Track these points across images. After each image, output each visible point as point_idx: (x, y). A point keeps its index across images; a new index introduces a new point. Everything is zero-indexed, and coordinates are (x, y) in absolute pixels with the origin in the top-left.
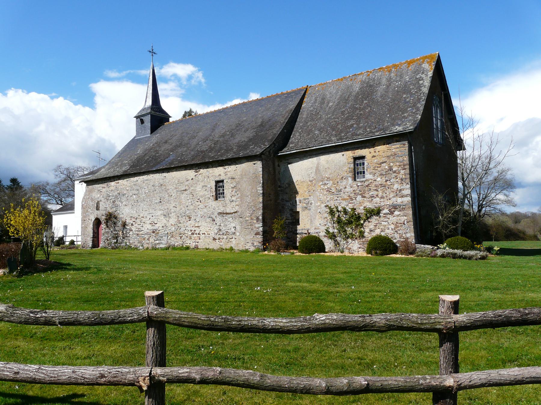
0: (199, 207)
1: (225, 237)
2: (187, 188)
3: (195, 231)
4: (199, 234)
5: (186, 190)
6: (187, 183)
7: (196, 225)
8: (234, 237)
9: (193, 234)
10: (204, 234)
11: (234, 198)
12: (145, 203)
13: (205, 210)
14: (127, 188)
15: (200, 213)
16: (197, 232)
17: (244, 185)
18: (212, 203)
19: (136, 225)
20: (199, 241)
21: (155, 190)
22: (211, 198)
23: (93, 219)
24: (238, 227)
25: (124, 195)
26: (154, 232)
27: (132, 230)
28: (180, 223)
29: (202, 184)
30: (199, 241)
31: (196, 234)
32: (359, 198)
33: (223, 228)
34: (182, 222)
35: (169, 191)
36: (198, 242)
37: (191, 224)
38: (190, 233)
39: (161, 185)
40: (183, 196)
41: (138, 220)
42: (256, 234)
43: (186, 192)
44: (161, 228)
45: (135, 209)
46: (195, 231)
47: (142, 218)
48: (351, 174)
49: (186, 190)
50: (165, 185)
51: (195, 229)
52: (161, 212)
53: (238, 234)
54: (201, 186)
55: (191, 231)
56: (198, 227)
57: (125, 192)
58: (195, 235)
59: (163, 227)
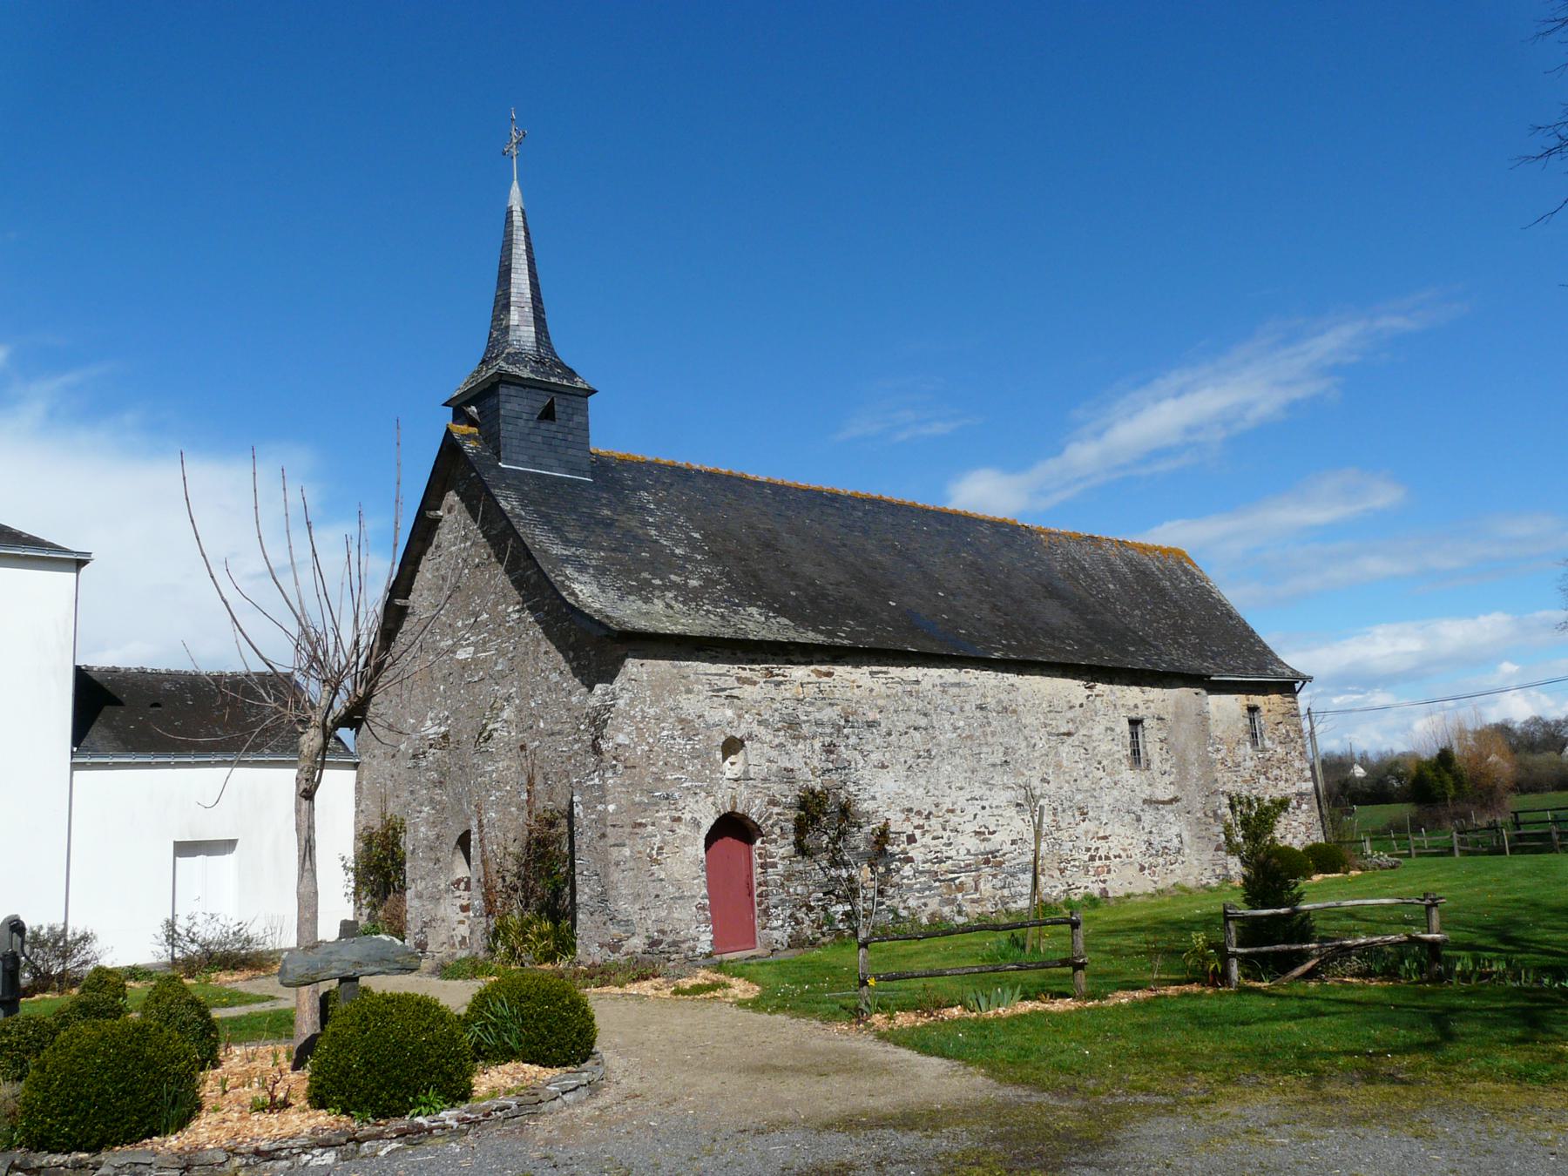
0: (1103, 783)
1: (1161, 860)
2: (1071, 727)
4: (1107, 858)
5: (1069, 734)
6: (1070, 715)
7: (1101, 834)
8: (1181, 858)
9: (1092, 858)
11: (1167, 767)
12: (957, 760)
13: (1116, 793)
14: (881, 702)
15: (1107, 800)
16: (1102, 853)
17: (1182, 739)
18: (1127, 775)
19: (928, 839)
20: (1107, 877)
21: (989, 724)
22: (1125, 761)
23: (708, 823)
24: (1186, 836)
25: (871, 725)
26: (987, 862)
27: (910, 860)
28: (1059, 829)
29: (1104, 723)
30: (1107, 877)
33: (1155, 840)
34: (1063, 825)
35: (1026, 732)
36: (1104, 882)
37: (1087, 832)
38: (1086, 858)
39: (1006, 709)
40: (1064, 750)
41: (933, 820)
43: (1069, 740)
44: (1007, 847)
45: (923, 782)
47: (948, 816)
48: (1248, 737)
49: (1069, 734)
52: (1010, 794)
53: (1187, 851)
54: (1102, 728)
55: (1088, 850)
56: (1105, 838)
57: (871, 716)
58: (1097, 863)
59: (1014, 842)
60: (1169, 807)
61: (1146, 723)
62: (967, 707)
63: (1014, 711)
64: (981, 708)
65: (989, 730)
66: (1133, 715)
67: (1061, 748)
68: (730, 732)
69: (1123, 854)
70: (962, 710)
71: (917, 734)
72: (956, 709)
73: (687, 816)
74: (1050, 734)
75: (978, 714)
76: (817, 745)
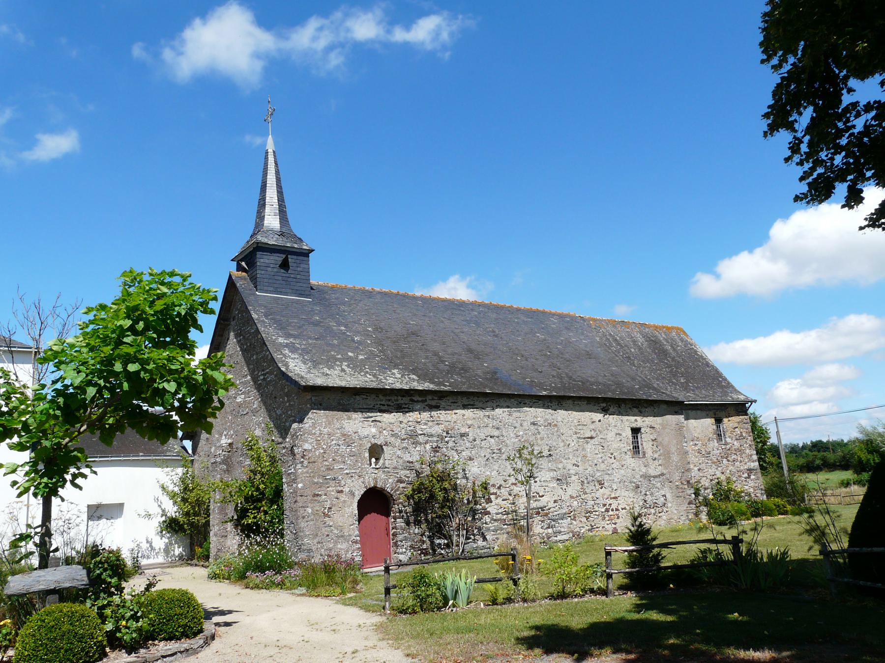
0: (614, 466)
1: (653, 511)
2: (593, 434)
3: (610, 504)
4: (617, 510)
5: (592, 438)
6: (592, 426)
7: (613, 496)
8: (665, 509)
9: (607, 510)
10: (625, 509)
11: (656, 456)
13: (622, 472)
14: (469, 422)
15: (617, 476)
16: (614, 506)
17: (666, 439)
19: (499, 500)
20: (617, 521)
21: (539, 433)
22: (629, 453)
23: (359, 493)
25: (462, 435)
26: (538, 513)
27: (488, 513)
28: (585, 493)
29: (615, 431)
30: (617, 521)
31: (612, 510)
32: (725, 461)
33: (649, 498)
35: (563, 437)
36: (615, 524)
37: (604, 494)
38: (603, 510)
40: (589, 447)
41: (503, 490)
42: (689, 503)
43: (592, 441)
44: (551, 505)
45: (496, 467)
46: (610, 504)
47: (512, 487)
49: (592, 438)
50: (556, 425)
51: (611, 501)
52: (552, 474)
53: (670, 505)
54: (613, 434)
55: (604, 505)
56: (615, 498)
57: (463, 430)
58: (611, 513)
59: (555, 502)
60: (657, 480)
61: (643, 430)
62: (525, 424)
63: (556, 425)
64: (534, 424)
65: (539, 436)
66: (634, 425)
67: (586, 446)
68: (373, 441)
69: (628, 508)
70: (521, 425)
71: (492, 440)
72: (518, 425)
73: (346, 489)
74: (579, 438)
75: (532, 427)
76: (428, 447)
